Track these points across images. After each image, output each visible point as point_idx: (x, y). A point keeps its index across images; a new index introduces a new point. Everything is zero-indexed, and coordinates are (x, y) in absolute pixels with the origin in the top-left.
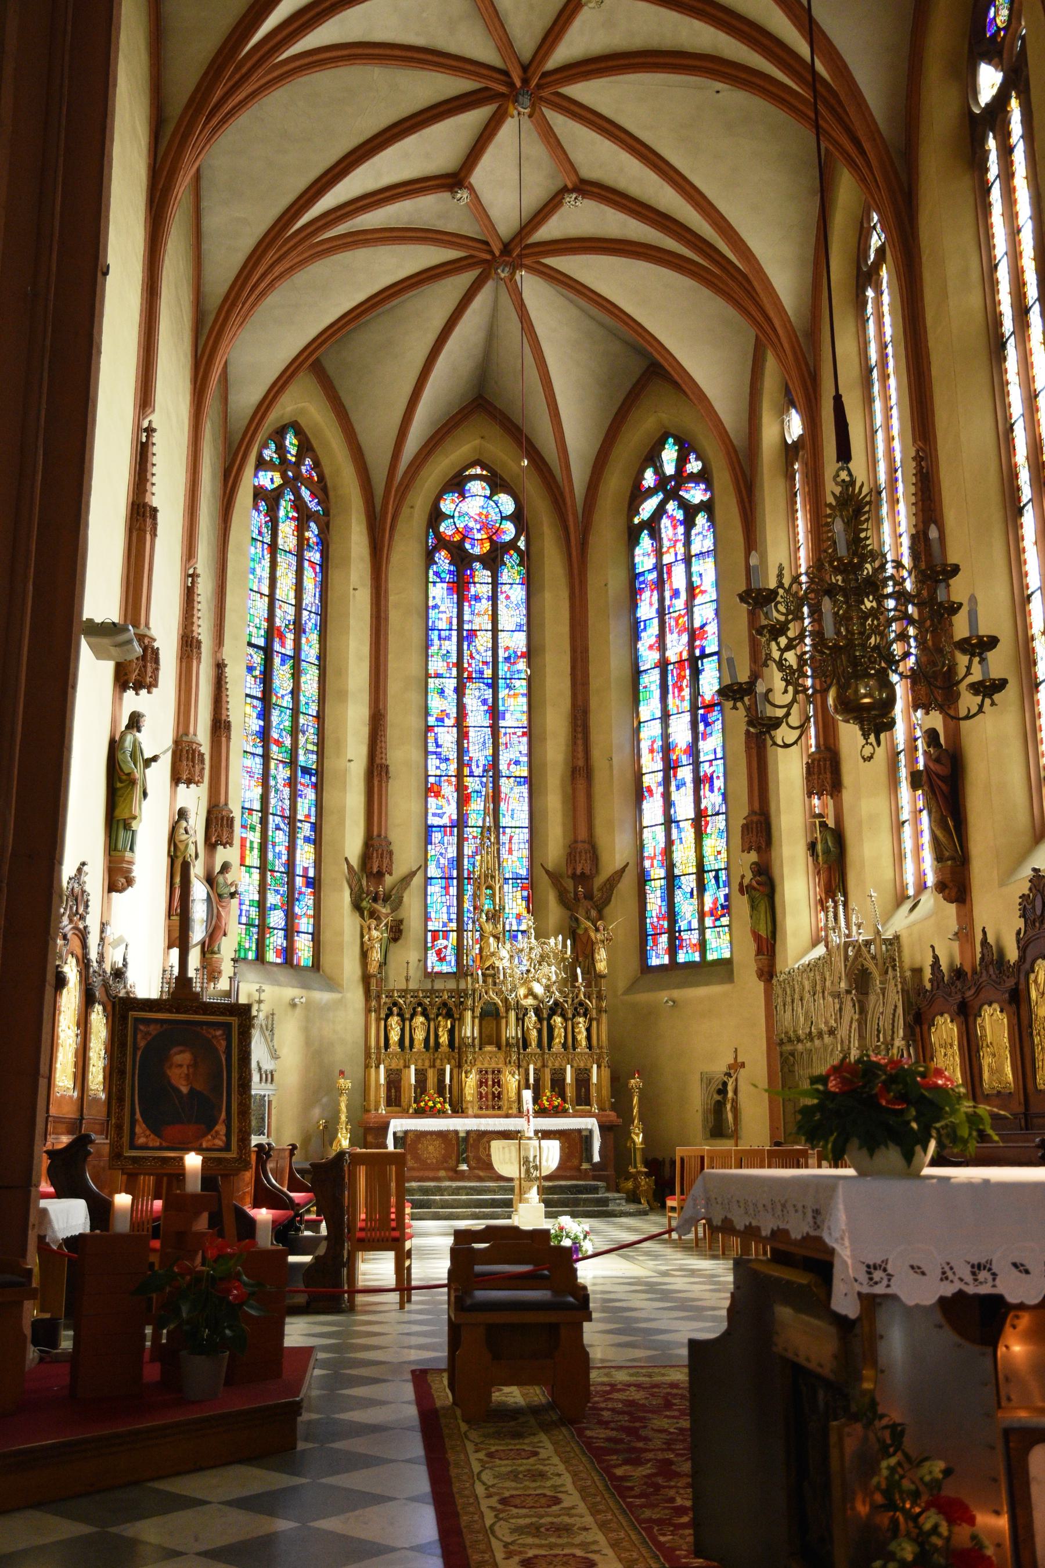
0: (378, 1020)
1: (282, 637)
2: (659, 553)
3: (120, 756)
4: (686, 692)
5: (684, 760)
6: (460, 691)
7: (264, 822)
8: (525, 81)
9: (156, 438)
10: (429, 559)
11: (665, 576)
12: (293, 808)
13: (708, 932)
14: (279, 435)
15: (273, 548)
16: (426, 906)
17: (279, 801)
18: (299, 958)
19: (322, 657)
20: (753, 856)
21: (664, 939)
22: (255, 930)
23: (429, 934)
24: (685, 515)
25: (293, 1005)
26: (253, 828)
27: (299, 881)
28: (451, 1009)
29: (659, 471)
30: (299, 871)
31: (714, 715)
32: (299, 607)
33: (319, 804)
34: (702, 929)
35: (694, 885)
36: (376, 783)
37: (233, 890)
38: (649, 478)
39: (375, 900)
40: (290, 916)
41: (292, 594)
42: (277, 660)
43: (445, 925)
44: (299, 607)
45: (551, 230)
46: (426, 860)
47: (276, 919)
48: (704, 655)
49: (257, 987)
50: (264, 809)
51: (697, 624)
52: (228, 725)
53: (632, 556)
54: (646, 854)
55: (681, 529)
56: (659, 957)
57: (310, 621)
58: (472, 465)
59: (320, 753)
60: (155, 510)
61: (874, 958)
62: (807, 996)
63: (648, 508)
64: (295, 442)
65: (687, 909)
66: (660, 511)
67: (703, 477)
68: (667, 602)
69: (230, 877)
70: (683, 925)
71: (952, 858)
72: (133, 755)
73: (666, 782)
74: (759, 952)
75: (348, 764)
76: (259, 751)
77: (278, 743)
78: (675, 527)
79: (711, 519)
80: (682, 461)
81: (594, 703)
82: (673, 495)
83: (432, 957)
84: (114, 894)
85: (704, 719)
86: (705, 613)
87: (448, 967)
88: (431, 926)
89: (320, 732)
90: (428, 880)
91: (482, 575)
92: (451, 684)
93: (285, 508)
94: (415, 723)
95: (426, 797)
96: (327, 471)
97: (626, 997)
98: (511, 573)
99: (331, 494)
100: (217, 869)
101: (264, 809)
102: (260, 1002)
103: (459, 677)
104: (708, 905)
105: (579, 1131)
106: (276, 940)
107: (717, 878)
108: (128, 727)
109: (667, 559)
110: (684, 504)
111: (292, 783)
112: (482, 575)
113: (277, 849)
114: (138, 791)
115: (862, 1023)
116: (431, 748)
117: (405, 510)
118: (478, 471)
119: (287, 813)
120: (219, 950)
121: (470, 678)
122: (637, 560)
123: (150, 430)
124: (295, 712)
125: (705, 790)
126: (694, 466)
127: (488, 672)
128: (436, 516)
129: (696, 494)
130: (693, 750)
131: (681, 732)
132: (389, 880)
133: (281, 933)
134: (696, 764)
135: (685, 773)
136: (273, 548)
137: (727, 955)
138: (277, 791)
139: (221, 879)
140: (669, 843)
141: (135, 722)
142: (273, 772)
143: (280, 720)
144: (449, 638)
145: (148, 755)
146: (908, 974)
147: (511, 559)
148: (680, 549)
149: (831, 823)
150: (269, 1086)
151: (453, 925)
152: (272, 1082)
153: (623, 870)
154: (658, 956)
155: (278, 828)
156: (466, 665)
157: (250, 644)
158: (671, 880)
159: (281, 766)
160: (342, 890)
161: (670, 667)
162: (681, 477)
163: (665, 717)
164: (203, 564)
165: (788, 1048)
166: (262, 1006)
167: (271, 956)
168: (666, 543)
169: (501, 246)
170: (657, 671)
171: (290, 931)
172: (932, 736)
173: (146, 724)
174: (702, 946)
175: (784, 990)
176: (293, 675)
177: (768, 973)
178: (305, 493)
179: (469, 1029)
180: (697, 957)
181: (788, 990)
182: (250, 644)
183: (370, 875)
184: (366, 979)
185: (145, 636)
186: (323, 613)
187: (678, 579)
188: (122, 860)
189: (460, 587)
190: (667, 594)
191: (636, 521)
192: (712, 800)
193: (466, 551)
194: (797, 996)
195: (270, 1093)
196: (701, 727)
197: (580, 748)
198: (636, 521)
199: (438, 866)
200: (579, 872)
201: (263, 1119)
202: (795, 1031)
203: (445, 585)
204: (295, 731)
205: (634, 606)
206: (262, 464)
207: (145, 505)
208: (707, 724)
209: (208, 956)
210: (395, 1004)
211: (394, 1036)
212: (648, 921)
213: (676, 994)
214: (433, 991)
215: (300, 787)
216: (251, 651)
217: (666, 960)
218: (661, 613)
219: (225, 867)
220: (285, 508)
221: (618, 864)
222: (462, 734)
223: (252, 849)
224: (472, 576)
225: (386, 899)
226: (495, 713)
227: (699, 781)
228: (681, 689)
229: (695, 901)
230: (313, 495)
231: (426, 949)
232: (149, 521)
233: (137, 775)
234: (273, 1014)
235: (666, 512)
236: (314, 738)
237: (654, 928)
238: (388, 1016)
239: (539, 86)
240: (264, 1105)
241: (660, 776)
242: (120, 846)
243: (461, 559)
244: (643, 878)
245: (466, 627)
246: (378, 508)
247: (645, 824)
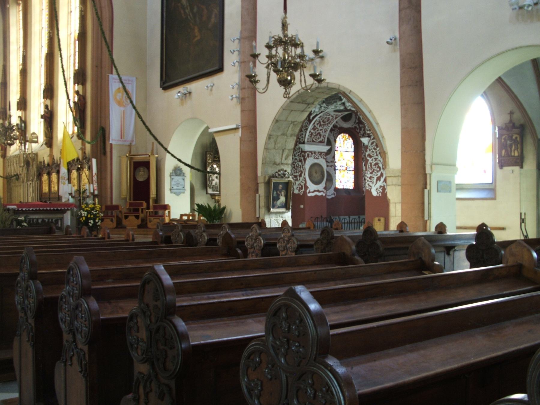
61: (31, 158)
62: (15, 164)
74: (2, 150)
115: (27, 174)
146: (38, 163)
175: (8, 161)
181: (10, 162)
194: (12, 164)
202: (11, 173)
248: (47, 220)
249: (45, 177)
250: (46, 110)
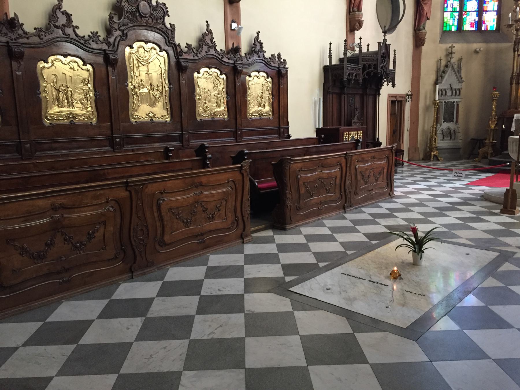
18: (487, 26)
22: (457, 14)
49: (450, 45)
102: (451, 53)
106: (471, 18)
120: (424, 29)
133: (475, 13)
152: (459, 95)
166: (453, 55)
167: (467, 27)
195: (457, 100)
201: (453, 114)
209: (417, 32)
234: (461, 59)
240: (454, 107)
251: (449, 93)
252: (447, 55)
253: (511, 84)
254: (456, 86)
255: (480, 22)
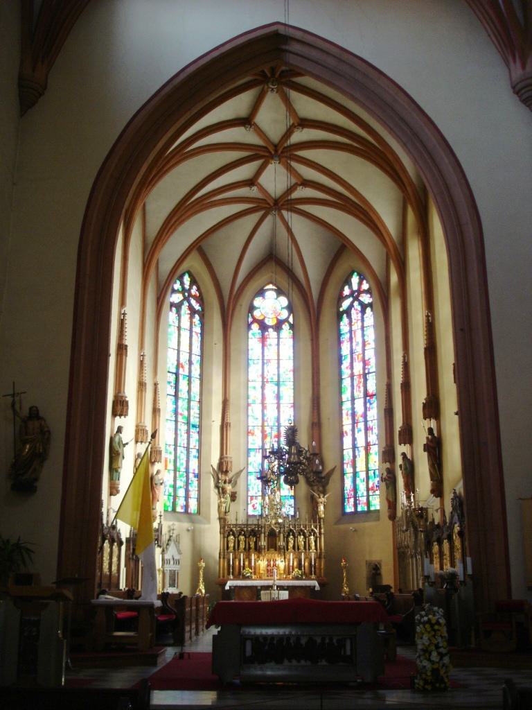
0: (224, 537)
1: (183, 367)
2: (350, 324)
3: (114, 444)
4: (362, 389)
5: (361, 419)
6: (263, 387)
7: (175, 450)
8: (276, 151)
9: (127, 317)
10: (249, 327)
11: (353, 336)
12: (188, 443)
13: (371, 498)
14: (181, 278)
15: (179, 328)
16: (248, 485)
17: (182, 440)
19: (201, 375)
20: (388, 465)
21: (352, 500)
22: (172, 498)
23: (249, 498)
24: (362, 308)
25: (188, 530)
26: (170, 453)
27: (191, 476)
28: (255, 533)
29: (350, 287)
30: (191, 471)
31: (372, 401)
32: (190, 354)
33: (200, 441)
34: (368, 496)
35: (365, 476)
36: (225, 429)
37: (161, 482)
38: (347, 291)
39: (225, 482)
40: (187, 491)
41: (188, 348)
42: (181, 378)
43: (256, 493)
44: (190, 354)
45: (295, 195)
46: (248, 464)
47: (181, 493)
48: (369, 373)
49: (171, 523)
50: (176, 445)
51: (366, 358)
52: (159, 410)
53: (339, 326)
54: (345, 462)
55: (360, 315)
56: (349, 508)
57: (196, 359)
58: (268, 284)
59: (201, 418)
60: (126, 346)
63: (345, 304)
64: (189, 279)
65: (362, 487)
66: (351, 306)
67: (368, 291)
68: (354, 348)
69: (160, 476)
70: (359, 493)
71: (436, 480)
72: (119, 443)
73: (353, 430)
74: (389, 508)
75: (213, 423)
76: (174, 419)
77: (181, 414)
78: (357, 314)
79: (372, 310)
80: (360, 284)
81: (322, 393)
82: (356, 299)
83: (250, 507)
84: (112, 497)
85: (369, 401)
86: (370, 354)
87: (258, 512)
88: (250, 494)
89: (201, 409)
90: (248, 473)
91: (272, 333)
92: (259, 385)
93: (185, 308)
94: (243, 403)
95: (248, 435)
96: (203, 291)
97: (336, 527)
98: (286, 331)
99: (205, 301)
100: (155, 473)
101: (176, 445)
102: (173, 530)
103: (263, 382)
104: (370, 486)
105: (309, 587)
106: (181, 502)
107: (374, 473)
108: (117, 432)
109: (354, 328)
110: (361, 303)
111: (188, 432)
112: (272, 333)
113: (181, 461)
114: (121, 456)
116: (250, 413)
117: (238, 307)
118: (270, 286)
119: (186, 446)
121: (267, 382)
122: (341, 328)
123: (124, 314)
124: (189, 401)
125: (369, 433)
126: (365, 286)
127: (275, 379)
128: (252, 309)
129: (366, 299)
130: (365, 416)
131: (359, 405)
132: (231, 475)
134: (366, 422)
135: (361, 426)
136: (179, 328)
137: (378, 508)
138: (181, 436)
139: (156, 477)
140: (354, 457)
141: (120, 430)
142: (179, 427)
143: (182, 404)
144: (258, 363)
145: (124, 442)
147: (286, 327)
148: (360, 323)
149: (409, 456)
150: (177, 566)
151: (260, 494)
153: (334, 469)
154: (350, 507)
155: (182, 452)
156: (265, 375)
157: (169, 372)
158: (355, 474)
159: (183, 424)
160: (210, 479)
161: (355, 377)
162: (360, 292)
163: (353, 399)
164: (148, 350)
165: (402, 550)
167: (179, 509)
168: (354, 321)
169: (273, 201)
170: (349, 379)
171: (187, 497)
172: (430, 430)
173: (124, 431)
174: (368, 503)
176: (188, 384)
177: (393, 516)
178: (193, 302)
179: (263, 543)
180: (366, 509)
182: (169, 372)
183: (222, 472)
184: (220, 519)
185: (122, 397)
186: (202, 356)
187: (358, 338)
188: (114, 484)
189: (263, 339)
190: (354, 344)
191: (341, 309)
192: (373, 438)
193: (265, 324)
196: (368, 405)
197: (316, 414)
198: (341, 309)
199: (253, 467)
200: (314, 470)
203: (256, 340)
204: (189, 409)
205: (340, 349)
206: (174, 291)
207: (123, 345)
208: (371, 404)
210: (231, 530)
211: (231, 545)
212: (346, 492)
213: (355, 525)
214: (247, 525)
215: (191, 433)
216: (169, 374)
217: (353, 510)
218: (352, 352)
219: (158, 472)
220: (185, 308)
221: (332, 468)
222: (264, 407)
223: (170, 462)
224: (269, 335)
225: (230, 482)
226: (278, 397)
227: (367, 429)
228: (359, 387)
229: (365, 483)
230: (197, 302)
231: (248, 504)
232: (124, 351)
233: (120, 451)
235: (353, 306)
236: (198, 411)
237: (348, 495)
238: (228, 536)
239: (282, 152)
241: (350, 427)
242: (114, 479)
243: (263, 327)
244: (343, 474)
245: (266, 358)
246: (226, 306)
247: (344, 448)
248: (319, 640)
249: (436, 548)
250: (430, 437)
251: (172, 562)
252: (169, 531)
253: (220, 558)
254: (177, 557)
255: (187, 506)
